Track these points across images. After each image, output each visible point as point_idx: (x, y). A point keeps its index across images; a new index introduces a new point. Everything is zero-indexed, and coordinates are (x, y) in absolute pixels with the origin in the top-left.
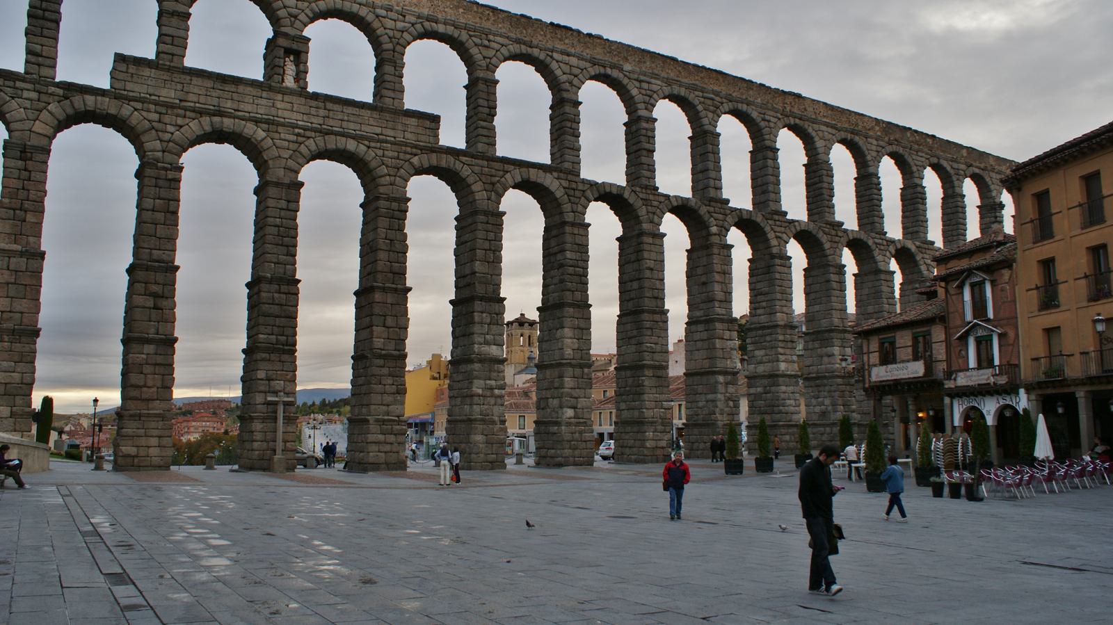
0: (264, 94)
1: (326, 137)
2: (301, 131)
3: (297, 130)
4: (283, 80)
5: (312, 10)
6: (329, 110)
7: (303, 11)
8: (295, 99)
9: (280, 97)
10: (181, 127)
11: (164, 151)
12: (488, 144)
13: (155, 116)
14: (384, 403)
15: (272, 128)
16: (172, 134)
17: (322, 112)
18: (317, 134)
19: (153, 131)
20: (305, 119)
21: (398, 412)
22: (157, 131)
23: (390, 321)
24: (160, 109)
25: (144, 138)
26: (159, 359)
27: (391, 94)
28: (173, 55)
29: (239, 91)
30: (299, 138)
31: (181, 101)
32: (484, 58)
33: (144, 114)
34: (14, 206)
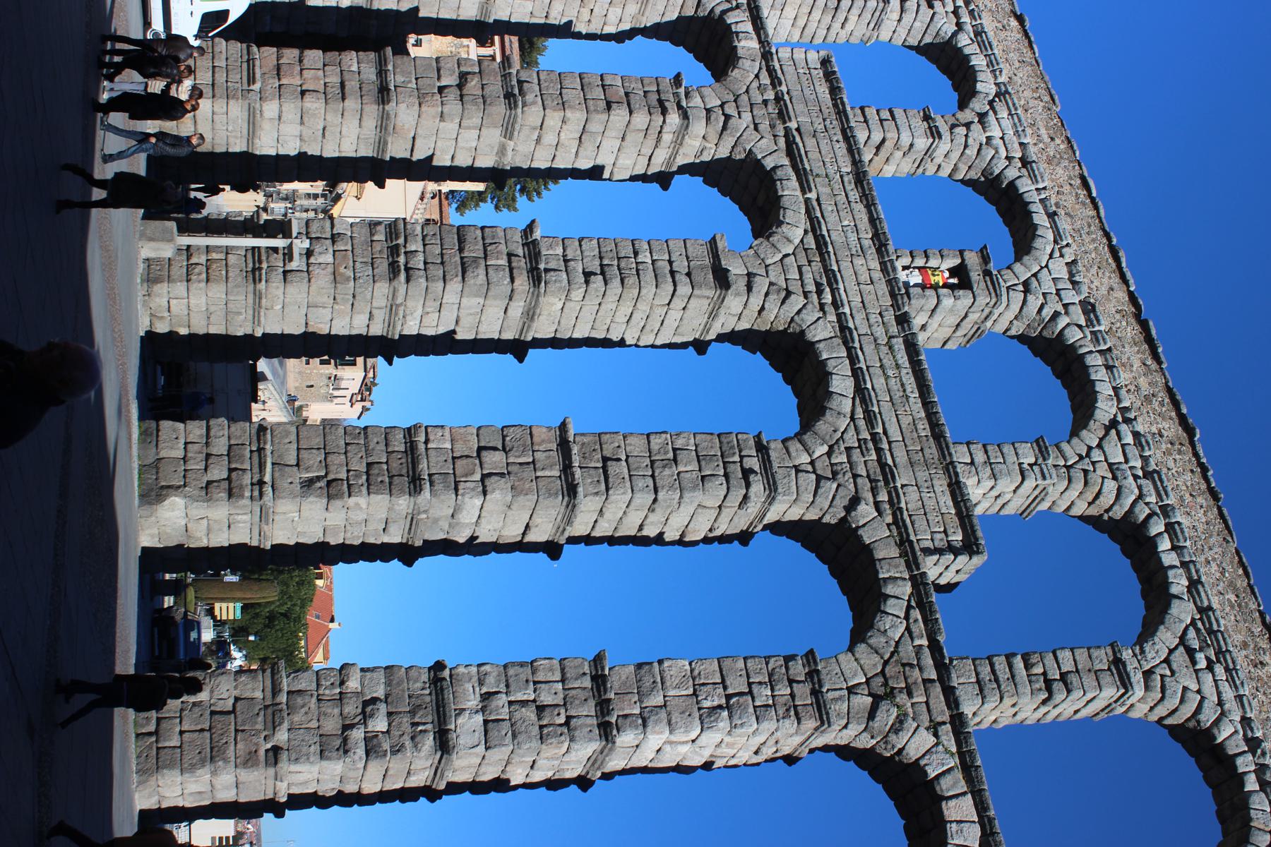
0: (867, 243)
4: (905, 268)
8: (883, 288)
9: (875, 264)
10: (756, 129)
12: (978, 682)
14: (304, 454)
17: (879, 331)
20: (853, 304)
21: (283, 484)
23: (494, 460)
26: (352, 85)
27: (980, 458)
28: (866, 121)
31: (798, 130)
32: (1167, 661)
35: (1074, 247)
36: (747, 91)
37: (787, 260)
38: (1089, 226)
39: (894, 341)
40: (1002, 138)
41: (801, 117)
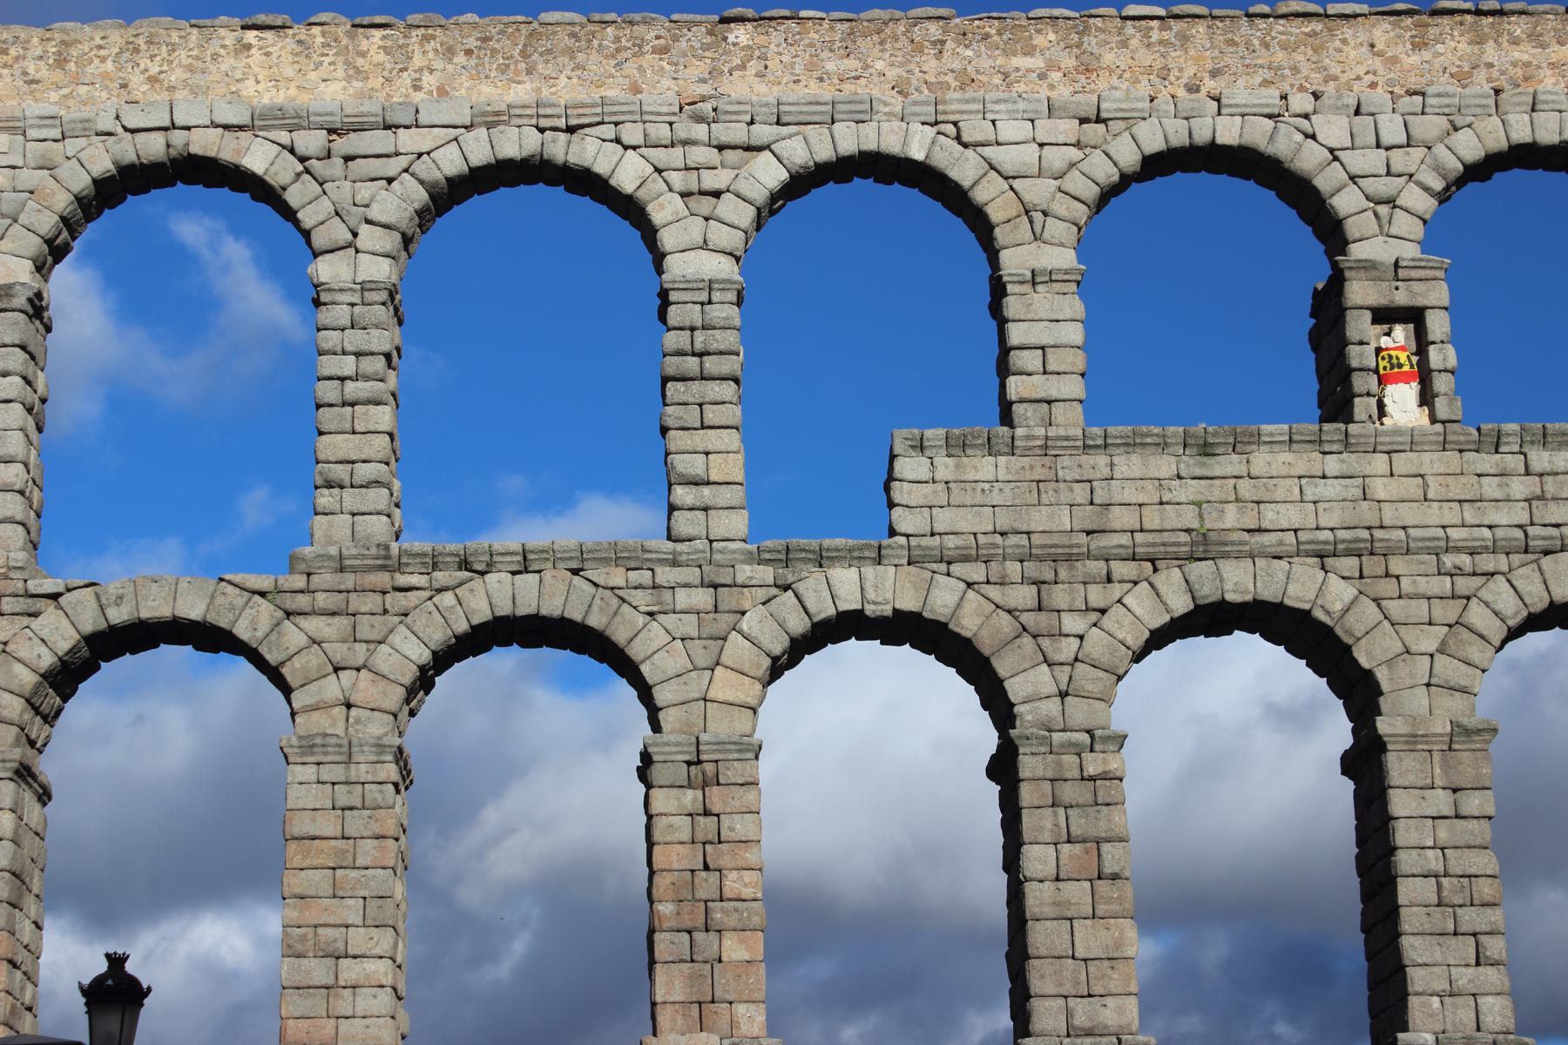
0: (1332, 464)
1: (1546, 562)
2: (1465, 560)
3: (1449, 560)
4: (1382, 412)
5: (1438, 169)
6: (1541, 475)
7: (1411, 176)
8: (1431, 461)
9: (1380, 463)
10: (1103, 611)
11: (1063, 695)
13: (1023, 596)
15: (1373, 565)
16: (1081, 637)
17: (1520, 487)
18: (1516, 559)
19: (1027, 640)
20: (1469, 519)
22: (1035, 637)
24: (1032, 569)
25: (1002, 667)
28: (1049, 402)
29: (1254, 472)
30: (1459, 581)
31: (1089, 533)
33: (993, 592)
34: (688, 924)
35: (1286, 88)
36: (1009, 612)
37: (1395, 616)
38: (1235, 44)
39: (1536, 466)
40: (1041, 145)
41: (1053, 519)
